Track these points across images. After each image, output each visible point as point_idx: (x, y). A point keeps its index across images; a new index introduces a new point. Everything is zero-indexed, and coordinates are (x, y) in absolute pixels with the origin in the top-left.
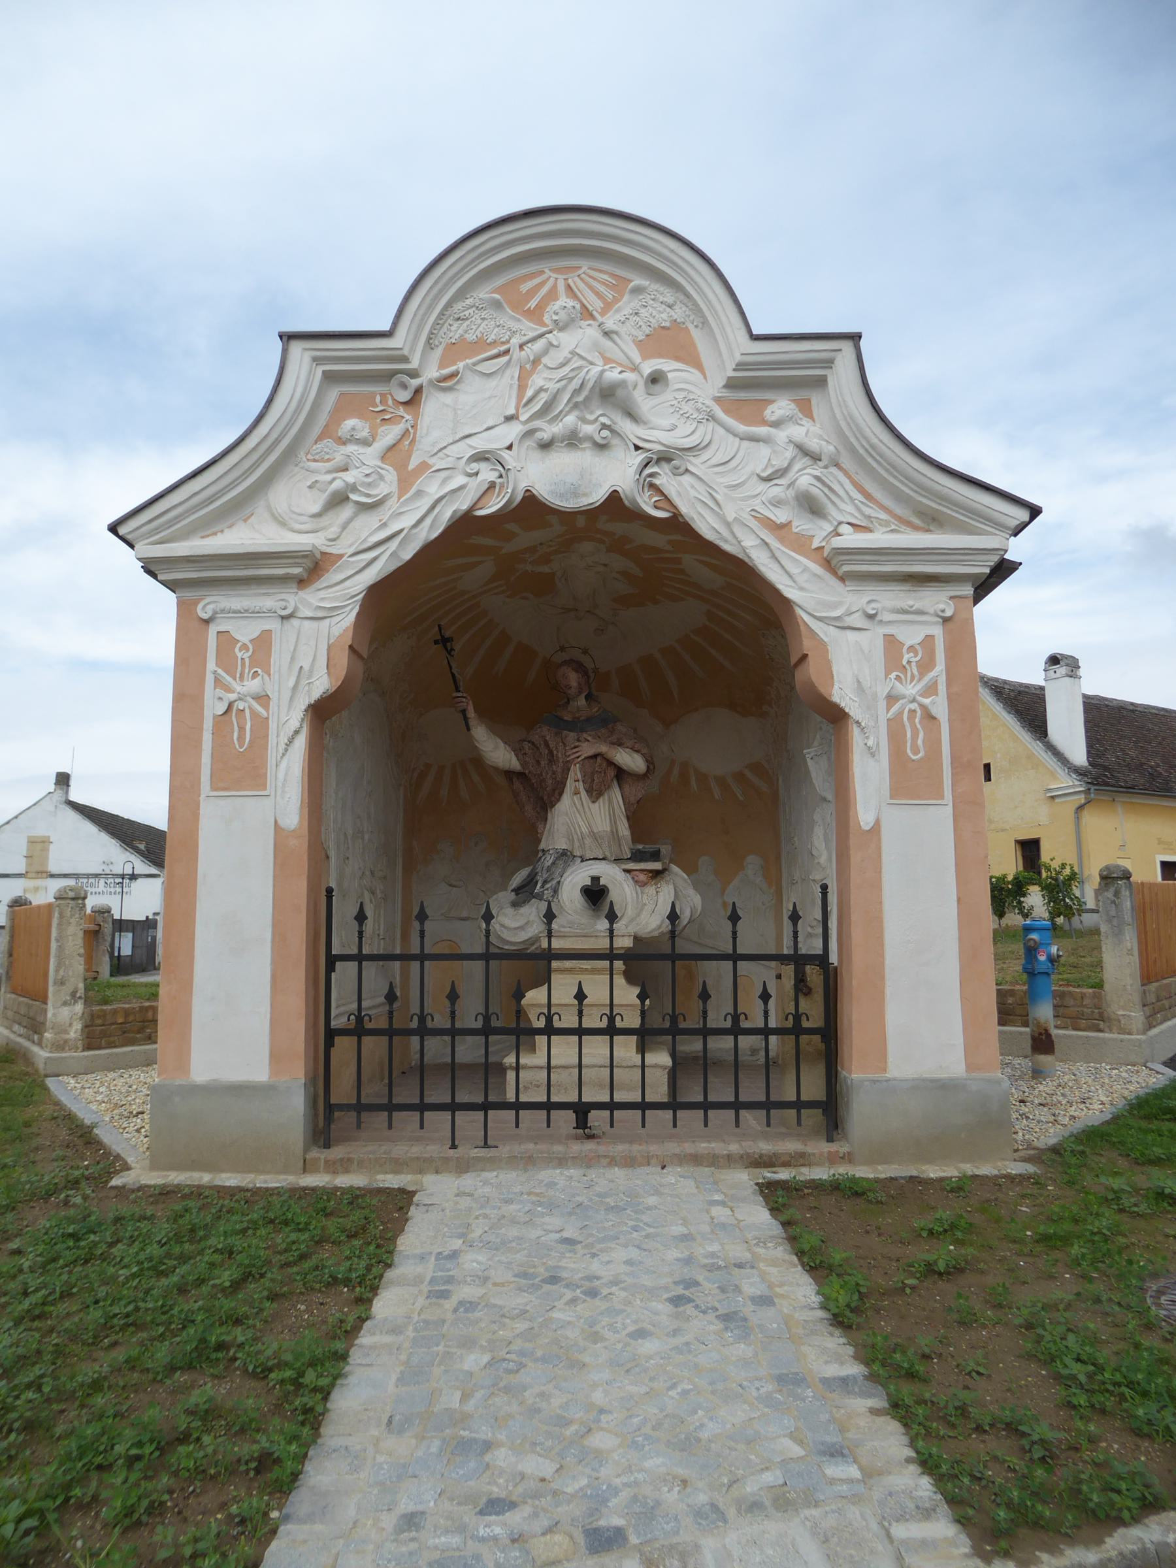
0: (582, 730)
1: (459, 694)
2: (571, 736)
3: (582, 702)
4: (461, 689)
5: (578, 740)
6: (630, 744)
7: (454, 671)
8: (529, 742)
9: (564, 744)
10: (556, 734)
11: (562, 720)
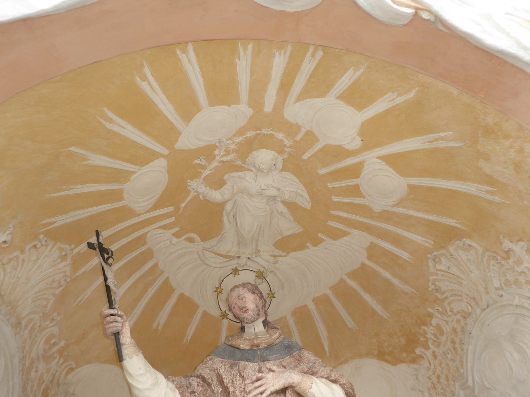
0: (264, 360)
1: (112, 312)
2: (250, 368)
3: (259, 327)
4: (116, 306)
5: (260, 371)
6: (325, 371)
7: (110, 283)
8: (198, 377)
9: (242, 377)
10: (232, 366)
11: (239, 349)
